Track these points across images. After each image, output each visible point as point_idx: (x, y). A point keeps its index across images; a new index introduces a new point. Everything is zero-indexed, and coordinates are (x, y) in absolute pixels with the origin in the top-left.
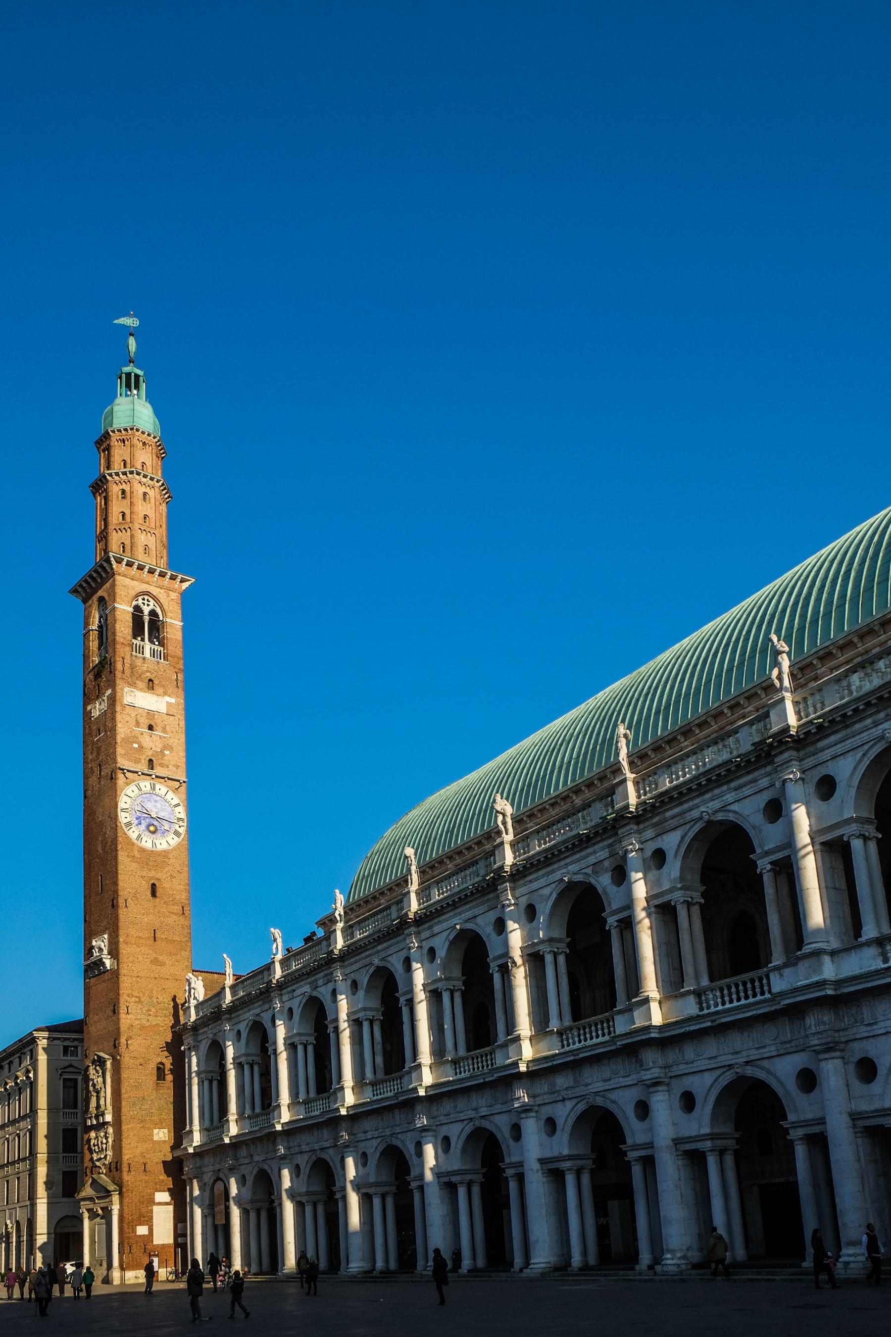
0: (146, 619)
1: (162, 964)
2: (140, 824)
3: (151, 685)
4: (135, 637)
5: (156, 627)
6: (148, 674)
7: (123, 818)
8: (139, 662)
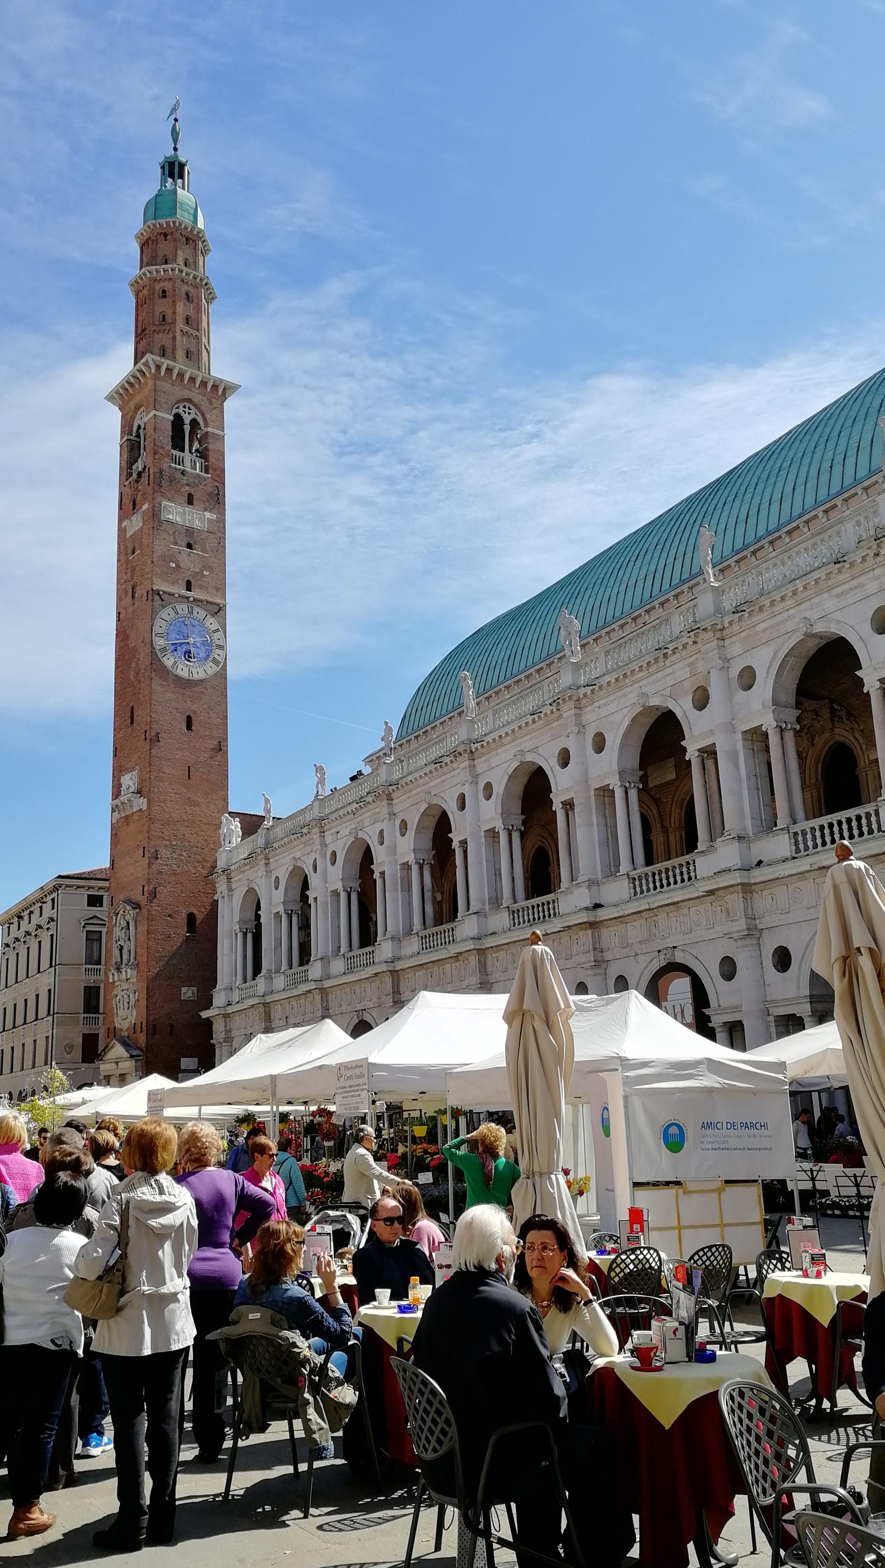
0: (187, 428)
1: (197, 804)
2: (176, 650)
3: (190, 501)
4: (174, 447)
6: (187, 488)
7: (160, 642)
8: (178, 475)
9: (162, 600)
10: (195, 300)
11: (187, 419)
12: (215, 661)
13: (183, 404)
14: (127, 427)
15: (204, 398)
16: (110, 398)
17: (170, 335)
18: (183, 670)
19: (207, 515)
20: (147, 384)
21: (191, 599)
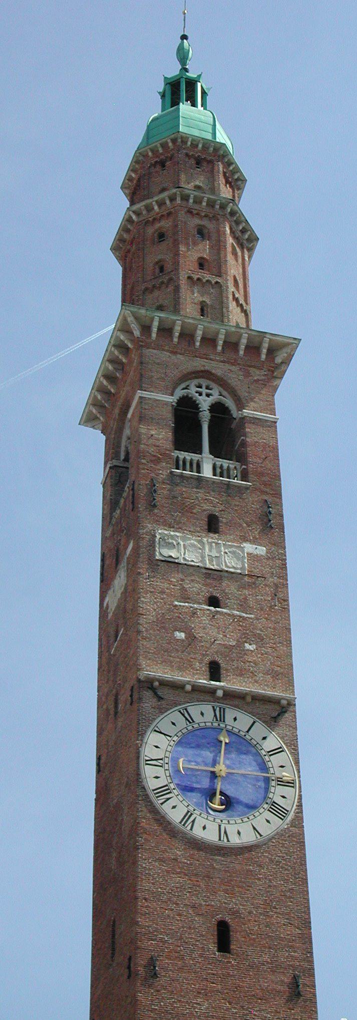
3: (213, 525)
4: (179, 444)
5: (227, 435)
9: (160, 698)
10: (214, 237)
11: (205, 403)
12: (275, 809)
13: (196, 382)
14: (112, 450)
15: (233, 368)
16: (89, 420)
17: (171, 288)
18: (207, 828)
19: (249, 547)
20: (130, 362)
21: (220, 693)
